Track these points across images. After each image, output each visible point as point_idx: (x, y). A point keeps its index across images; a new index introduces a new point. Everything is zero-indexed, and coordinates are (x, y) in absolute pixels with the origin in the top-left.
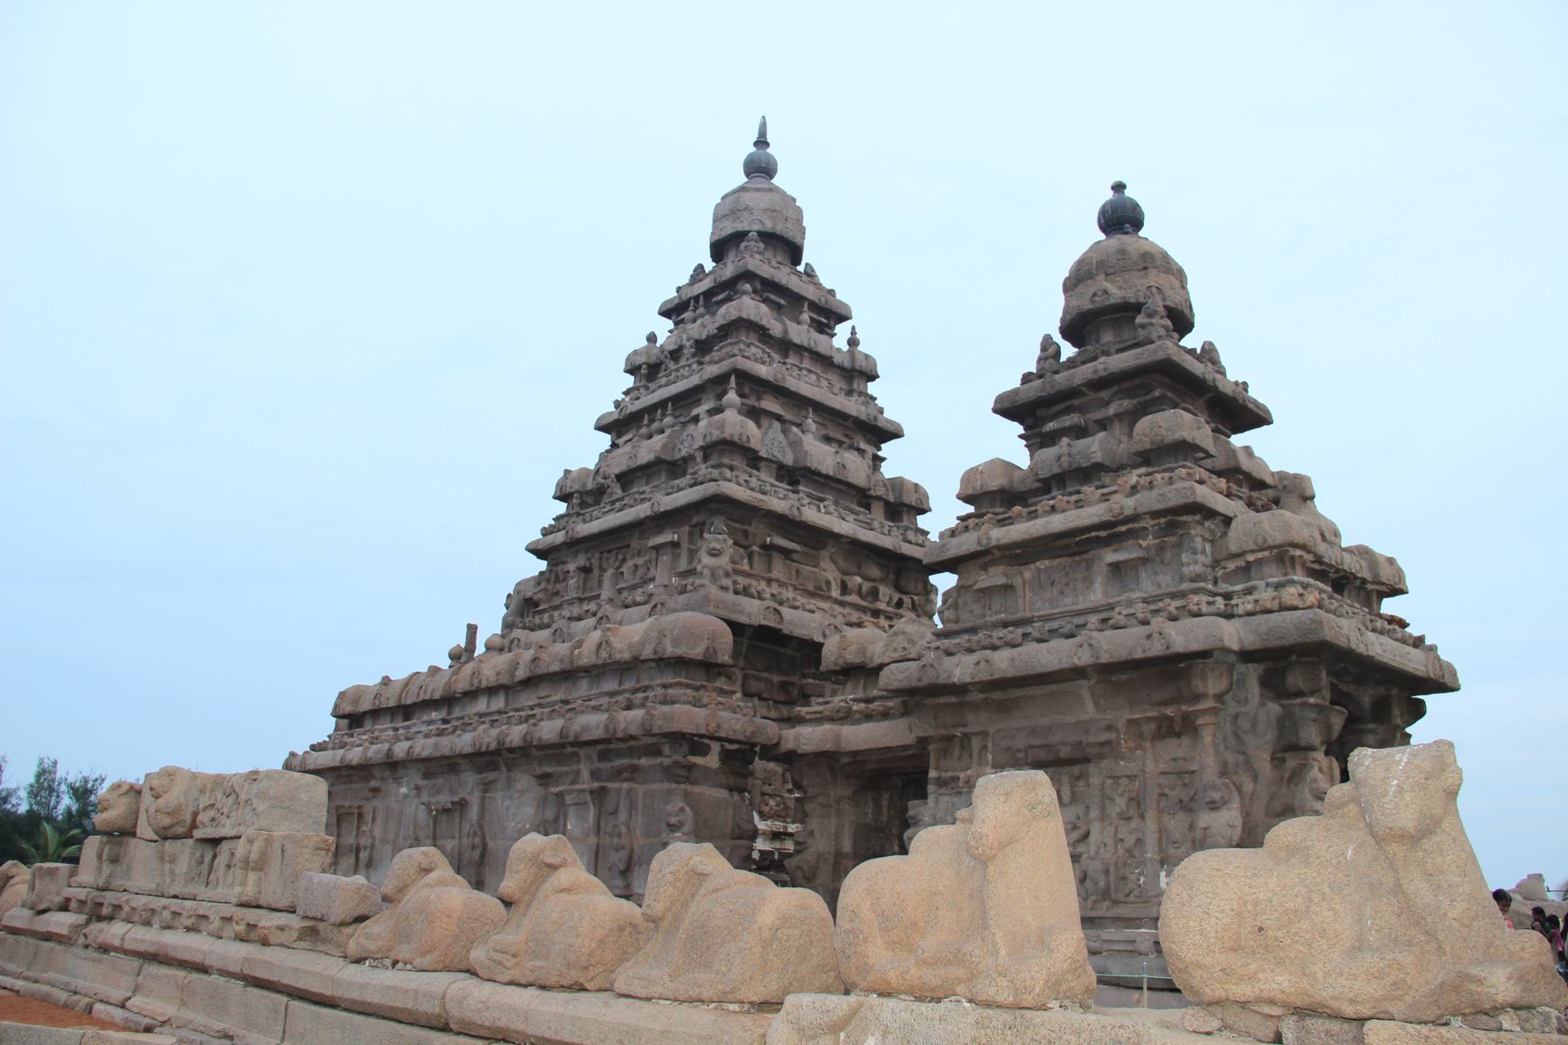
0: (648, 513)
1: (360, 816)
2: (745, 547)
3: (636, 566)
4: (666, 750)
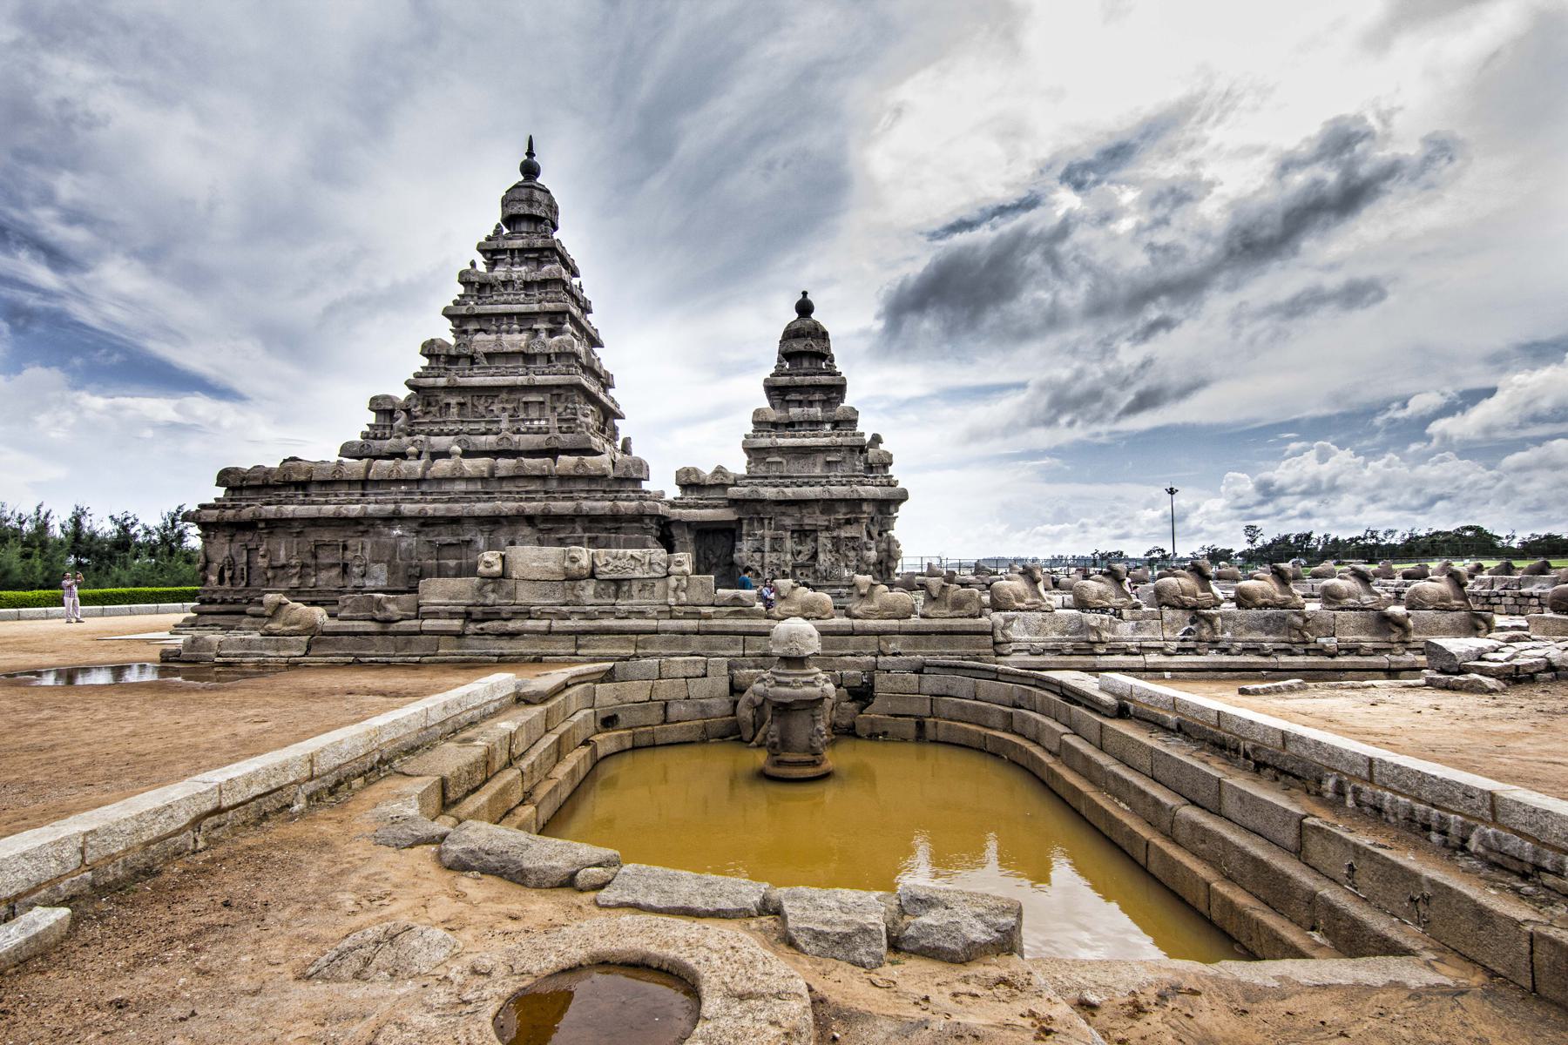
0: (525, 383)
1: (345, 548)
4: (647, 521)
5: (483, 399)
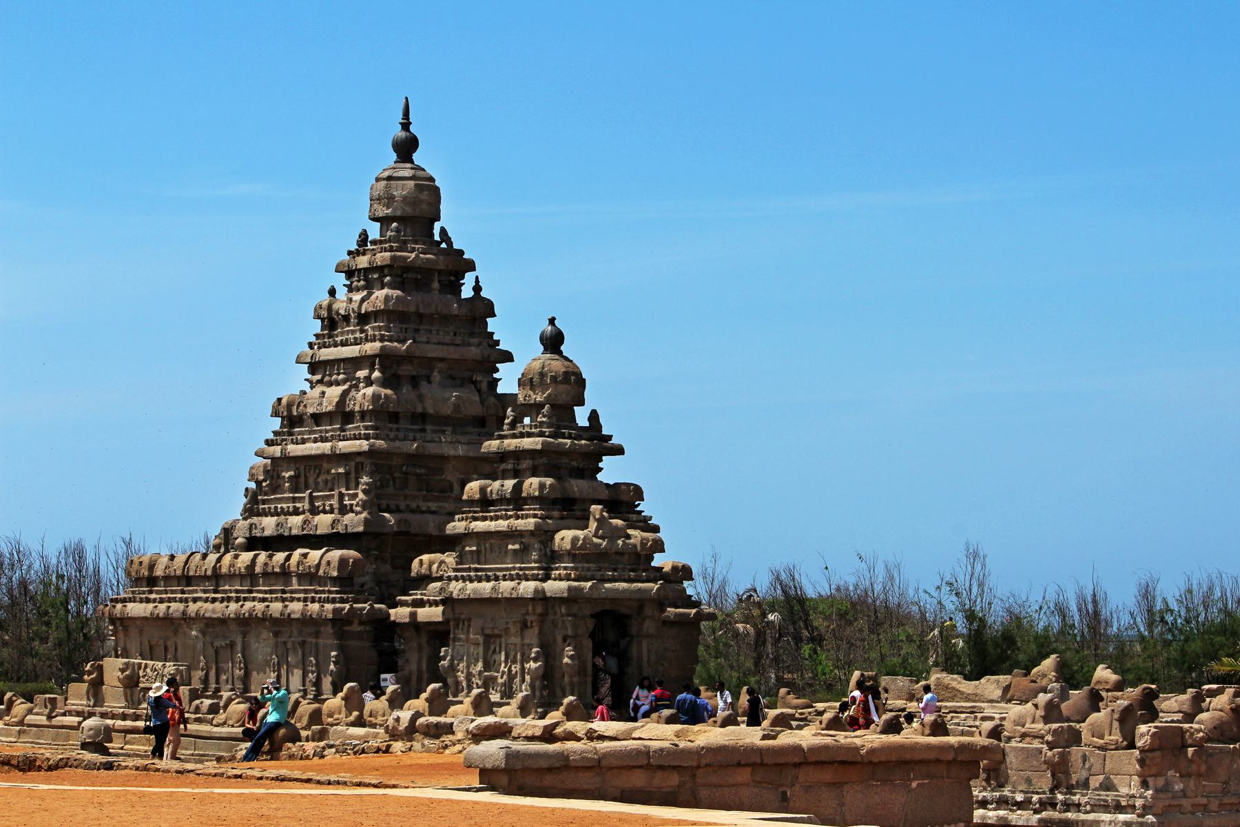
0: (330, 452)
2: (392, 475)
3: (326, 482)
5: (313, 468)
